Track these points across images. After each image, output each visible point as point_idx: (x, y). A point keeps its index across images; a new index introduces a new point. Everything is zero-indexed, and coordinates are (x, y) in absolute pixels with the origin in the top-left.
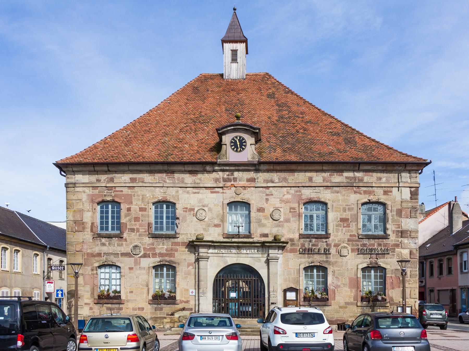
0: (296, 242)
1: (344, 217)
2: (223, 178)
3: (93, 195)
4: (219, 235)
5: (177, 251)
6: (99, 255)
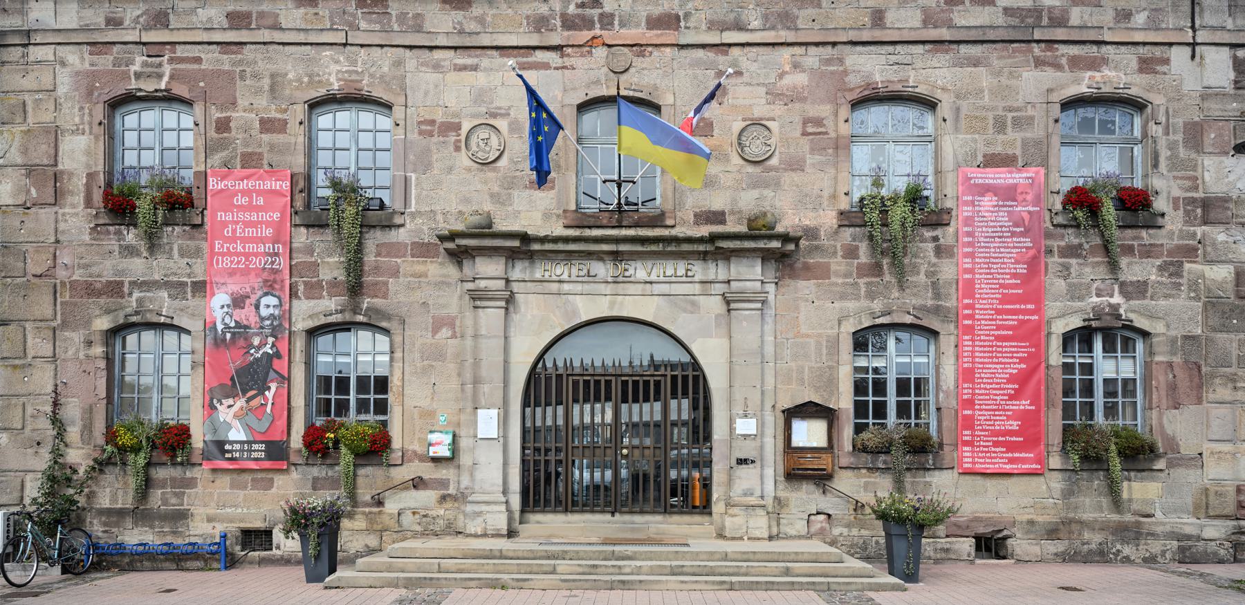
0: (824, 241)
1: (998, 149)
2: (564, 16)
3: (93, 75)
4: (547, 216)
5: (396, 273)
6: (115, 289)
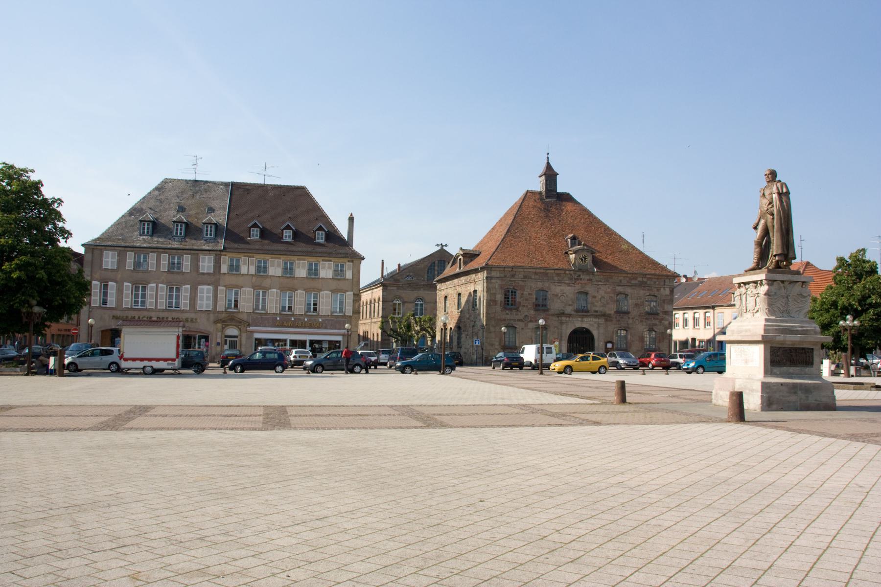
6: (504, 320)
